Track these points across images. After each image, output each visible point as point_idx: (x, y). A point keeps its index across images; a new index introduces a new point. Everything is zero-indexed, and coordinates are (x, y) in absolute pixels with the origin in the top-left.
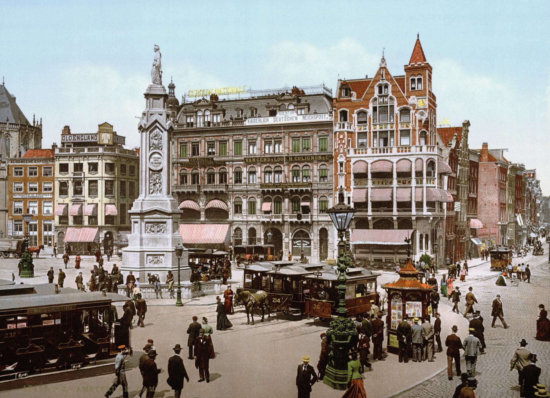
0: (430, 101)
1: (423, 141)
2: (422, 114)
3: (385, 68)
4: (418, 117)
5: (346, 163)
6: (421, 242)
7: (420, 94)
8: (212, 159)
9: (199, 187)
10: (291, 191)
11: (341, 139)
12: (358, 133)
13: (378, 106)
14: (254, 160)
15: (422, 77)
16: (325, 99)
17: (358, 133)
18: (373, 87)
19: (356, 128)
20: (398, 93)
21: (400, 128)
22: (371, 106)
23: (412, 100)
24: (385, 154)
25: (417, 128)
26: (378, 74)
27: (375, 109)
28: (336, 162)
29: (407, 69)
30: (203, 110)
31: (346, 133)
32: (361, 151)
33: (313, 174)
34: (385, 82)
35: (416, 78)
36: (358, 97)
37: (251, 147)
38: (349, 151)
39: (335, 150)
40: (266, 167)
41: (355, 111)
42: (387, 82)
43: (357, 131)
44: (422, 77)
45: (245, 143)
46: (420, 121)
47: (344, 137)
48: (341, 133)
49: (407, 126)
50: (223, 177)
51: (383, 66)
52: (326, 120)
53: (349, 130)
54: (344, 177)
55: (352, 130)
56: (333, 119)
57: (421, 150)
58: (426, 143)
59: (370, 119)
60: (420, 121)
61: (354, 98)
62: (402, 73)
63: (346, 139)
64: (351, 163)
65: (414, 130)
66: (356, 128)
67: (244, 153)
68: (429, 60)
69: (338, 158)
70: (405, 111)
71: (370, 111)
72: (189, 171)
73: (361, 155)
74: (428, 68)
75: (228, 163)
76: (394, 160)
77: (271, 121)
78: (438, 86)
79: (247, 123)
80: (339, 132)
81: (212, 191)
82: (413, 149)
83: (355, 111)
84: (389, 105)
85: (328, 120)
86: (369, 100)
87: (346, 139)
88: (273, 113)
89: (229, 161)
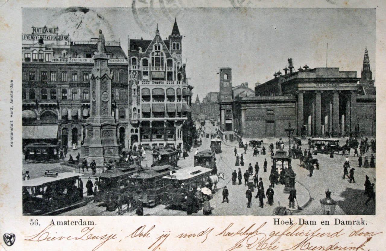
3: (159, 36)
5: (137, 89)
6: (178, 136)
9: (36, 101)
11: (135, 75)
14: (76, 85)
15: (179, 43)
18: (152, 46)
19: (142, 69)
20: (166, 51)
21: (167, 71)
22: (151, 56)
25: (177, 71)
26: (155, 39)
28: (130, 88)
30: (38, 49)
31: (137, 72)
32: (146, 83)
33: (115, 95)
36: (143, 51)
38: (138, 82)
39: (129, 81)
40: (84, 90)
41: (142, 59)
43: (142, 71)
44: (179, 43)
47: (136, 73)
48: (134, 71)
49: (171, 70)
51: (158, 34)
52: (124, 63)
53: (138, 70)
54: (136, 97)
55: (140, 70)
56: (128, 63)
60: (178, 67)
61: (141, 52)
63: (137, 75)
64: (140, 90)
65: (175, 72)
66: (142, 69)
69: (133, 86)
75: (57, 86)
76: (165, 89)
80: (133, 71)
81: (47, 105)
85: (126, 63)
86: (149, 53)
87: (137, 75)
89: (58, 85)
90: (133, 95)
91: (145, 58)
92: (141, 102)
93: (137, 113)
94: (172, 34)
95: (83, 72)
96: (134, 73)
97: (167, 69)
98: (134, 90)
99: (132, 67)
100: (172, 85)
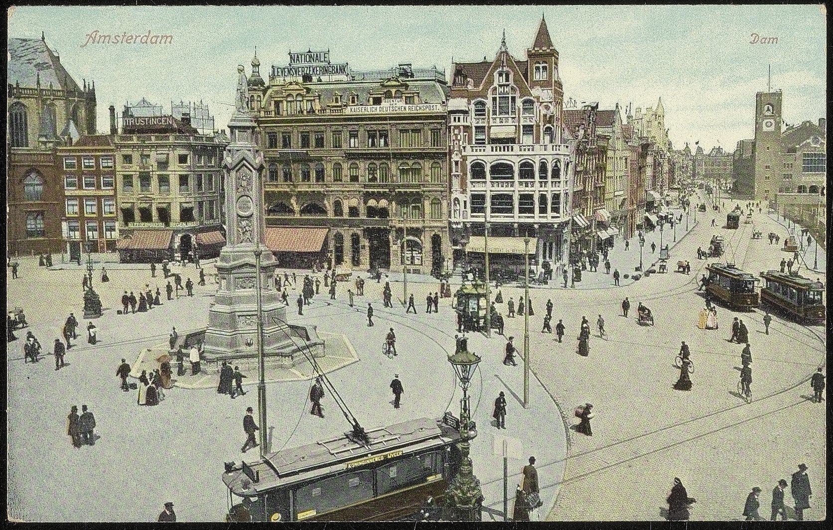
0: (556, 92)
1: (548, 138)
2: (547, 108)
4: (544, 112)
7: (545, 84)
8: (307, 153)
10: (400, 192)
12: (476, 127)
13: (498, 96)
16: (438, 85)
17: (476, 127)
21: (522, 123)
23: (536, 92)
24: (506, 153)
25: (542, 124)
27: (494, 99)
29: (530, 55)
34: (505, 69)
35: (541, 66)
36: (476, 85)
37: (352, 140)
38: (464, 148)
41: (473, 102)
42: (508, 69)
43: (474, 124)
45: (345, 135)
46: (545, 116)
47: (460, 132)
50: (320, 175)
51: (503, 50)
53: (465, 124)
55: (468, 124)
57: (545, 150)
58: (551, 142)
59: (489, 111)
61: (470, 87)
62: (523, 57)
65: (538, 126)
67: (345, 146)
68: (557, 46)
70: (529, 104)
71: (489, 103)
72: (280, 167)
73: (478, 153)
74: (554, 54)
77: (377, 110)
78: (567, 71)
79: (348, 111)
82: (537, 146)
83: (473, 102)
84: (510, 95)
88: (377, 101)
90: (454, 173)
91: (480, 99)
92: (470, 187)
93: (462, 209)
94: (535, 46)
95: (368, 131)
96: (456, 131)
97: (522, 120)
98: (457, 163)
99: (452, 119)
100: (531, 153)
